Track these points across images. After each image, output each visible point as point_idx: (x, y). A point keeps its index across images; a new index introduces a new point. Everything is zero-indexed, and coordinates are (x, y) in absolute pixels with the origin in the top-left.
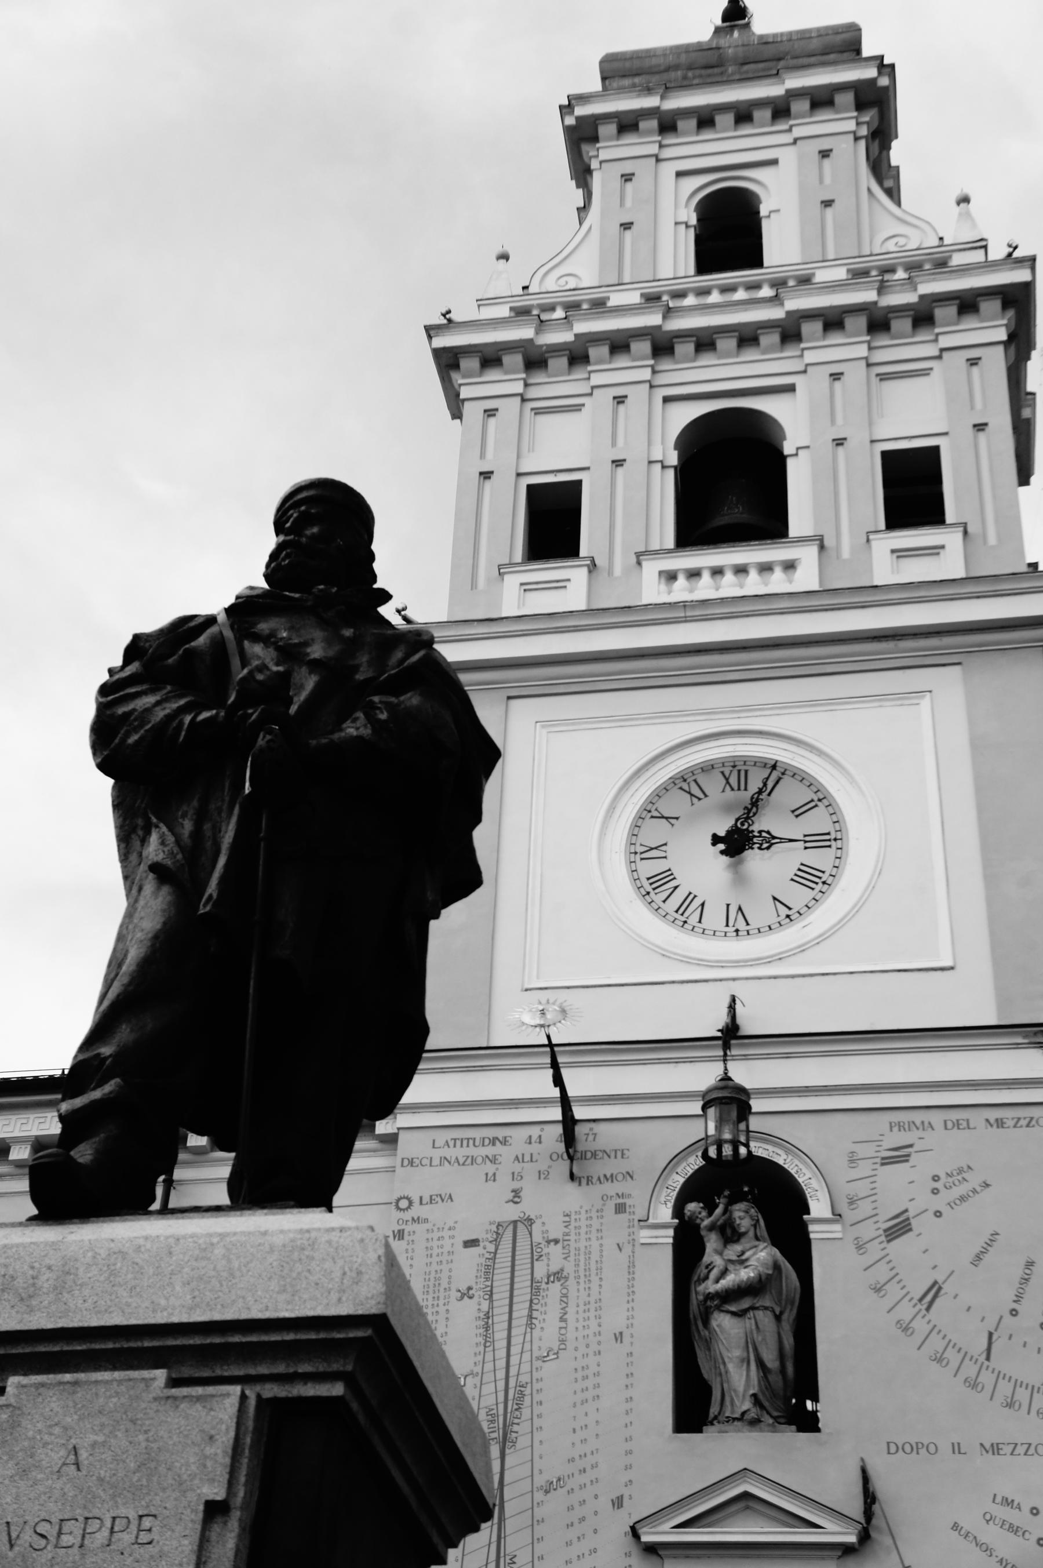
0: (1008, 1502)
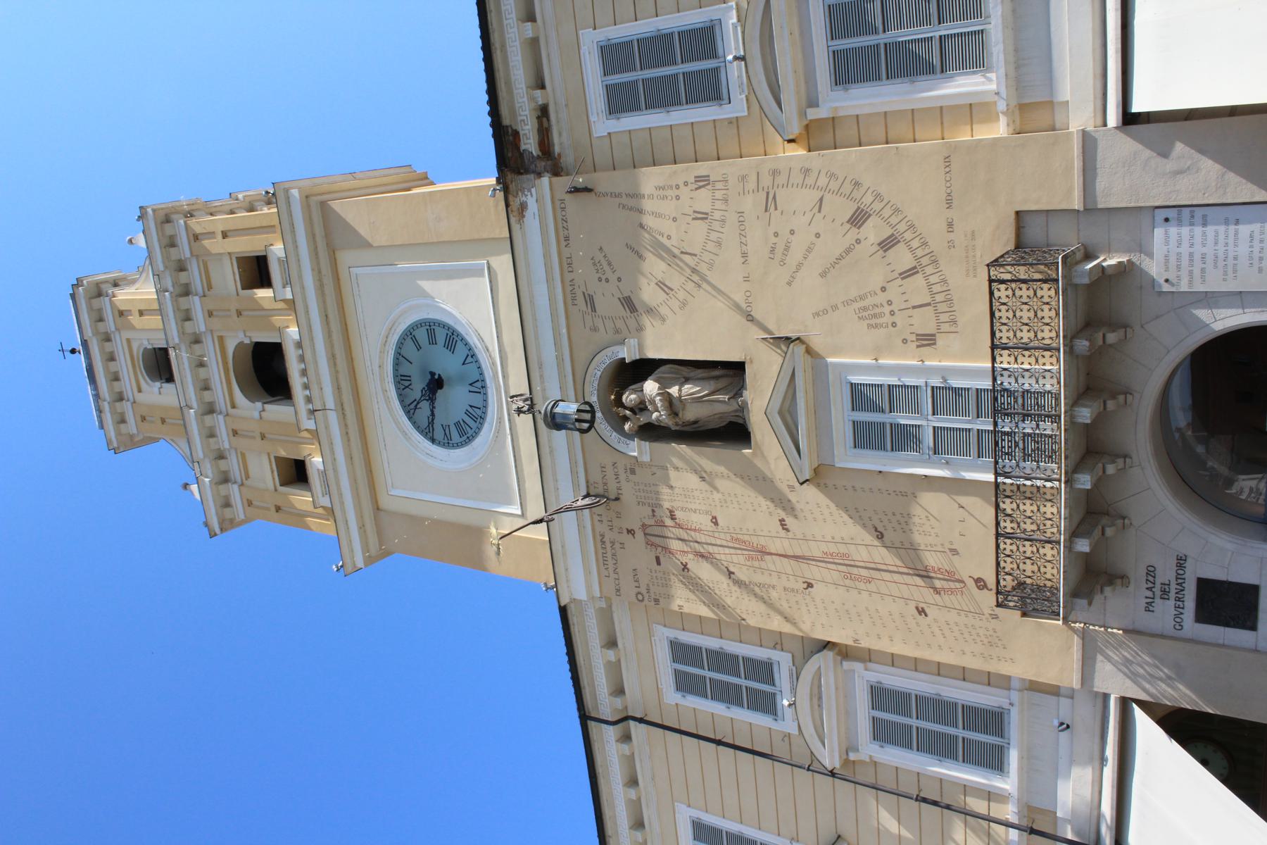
0: (773, 250)
